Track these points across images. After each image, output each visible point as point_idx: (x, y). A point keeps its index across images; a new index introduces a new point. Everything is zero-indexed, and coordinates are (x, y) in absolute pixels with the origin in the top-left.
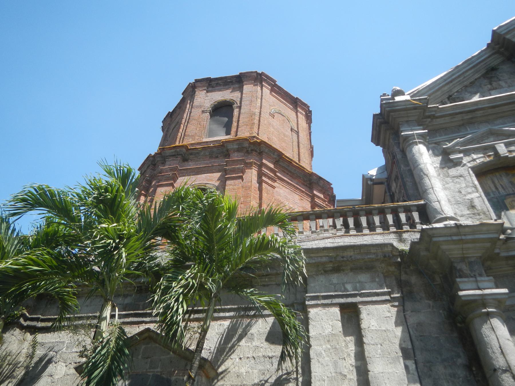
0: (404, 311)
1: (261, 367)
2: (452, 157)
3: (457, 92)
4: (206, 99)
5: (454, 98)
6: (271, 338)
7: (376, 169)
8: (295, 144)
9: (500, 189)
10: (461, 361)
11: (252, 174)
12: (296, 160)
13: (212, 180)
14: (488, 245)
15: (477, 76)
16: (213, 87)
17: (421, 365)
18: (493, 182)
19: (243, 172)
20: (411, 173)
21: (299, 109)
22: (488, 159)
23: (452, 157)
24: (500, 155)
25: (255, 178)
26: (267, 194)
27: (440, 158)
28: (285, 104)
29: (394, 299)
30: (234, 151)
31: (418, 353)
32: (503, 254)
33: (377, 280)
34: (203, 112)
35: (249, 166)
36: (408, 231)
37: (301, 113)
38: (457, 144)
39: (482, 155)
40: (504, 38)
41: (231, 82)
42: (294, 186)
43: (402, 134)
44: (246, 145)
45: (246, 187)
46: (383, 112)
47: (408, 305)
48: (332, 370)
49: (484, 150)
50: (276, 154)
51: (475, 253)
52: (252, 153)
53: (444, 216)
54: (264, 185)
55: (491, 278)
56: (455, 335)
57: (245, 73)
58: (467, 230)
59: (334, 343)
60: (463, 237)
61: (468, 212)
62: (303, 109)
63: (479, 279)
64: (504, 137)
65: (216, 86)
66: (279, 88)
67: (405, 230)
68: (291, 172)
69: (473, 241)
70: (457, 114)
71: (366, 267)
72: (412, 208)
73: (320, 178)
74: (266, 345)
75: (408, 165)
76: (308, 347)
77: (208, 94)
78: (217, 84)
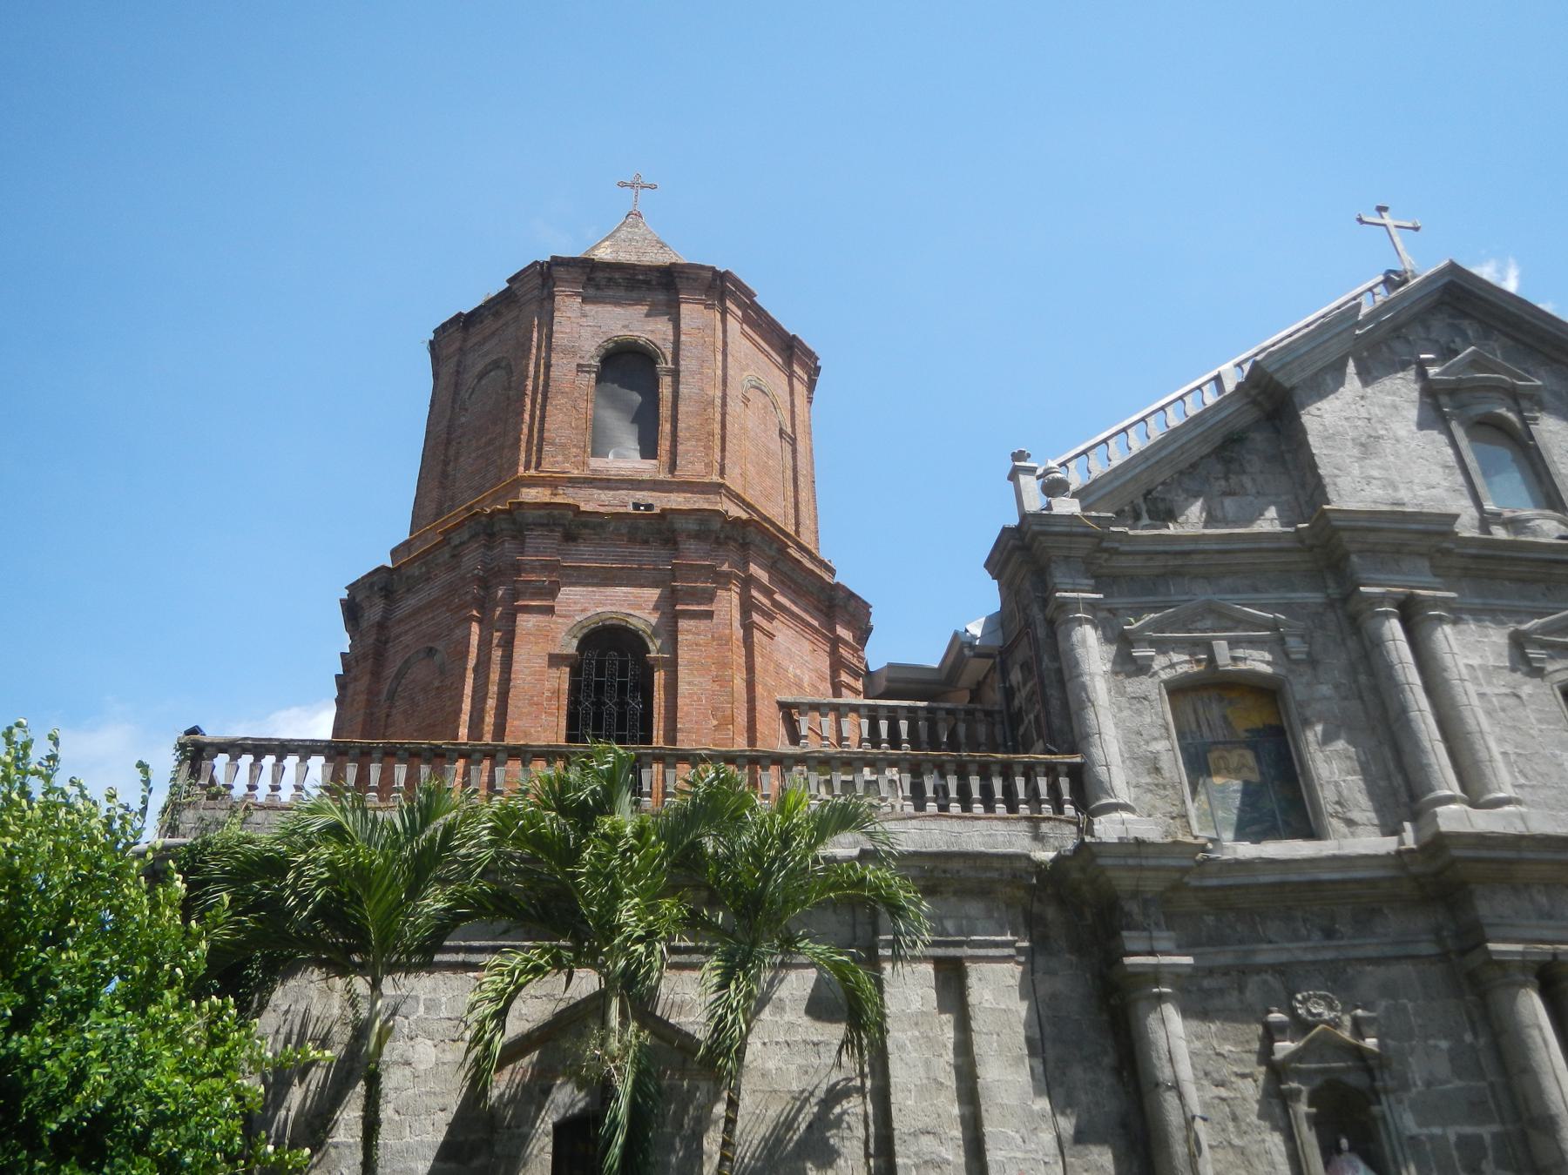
0: (1033, 972)
1: (800, 1061)
2: (1137, 653)
3: (1163, 483)
4: (584, 327)
6: (818, 1008)
8: (789, 473)
9: (1205, 728)
10: (1108, 1060)
11: (728, 603)
12: (791, 530)
13: (640, 607)
14: (1176, 876)
15: (1206, 450)
16: (598, 287)
18: (1195, 711)
19: (710, 597)
20: (1062, 683)
21: (796, 368)
22: (1196, 669)
23: (1137, 653)
24: (1217, 667)
25: (737, 616)
26: (763, 656)
27: (1114, 648)
28: (768, 355)
29: (1020, 951)
30: (689, 536)
31: (1048, 1045)
32: (1194, 883)
34: (580, 368)
35: (723, 580)
36: (1049, 819)
37: (800, 379)
38: (1146, 626)
39: (1187, 658)
41: (647, 282)
42: (803, 620)
44: (716, 525)
45: (720, 638)
46: (1025, 528)
47: (1040, 961)
48: (922, 1073)
49: (1192, 646)
50: (775, 546)
51: (1153, 885)
53: (1113, 801)
54: (757, 633)
55: (1172, 934)
56: (1105, 1017)
59: (926, 1028)
60: (1144, 862)
61: (1148, 780)
62: (804, 366)
63: (1155, 934)
64: (1230, 624)
65: (607, 286)
66: (759, 311)
67: (1045, 815)
68: (796, 583)
69: (1157, 869)
71: (982, 891)
73: (852, 595)
74: (806, 1020)
75: (1056, 656)
76: (883, 1031)
77: (587, 308)
78: (610, 280)
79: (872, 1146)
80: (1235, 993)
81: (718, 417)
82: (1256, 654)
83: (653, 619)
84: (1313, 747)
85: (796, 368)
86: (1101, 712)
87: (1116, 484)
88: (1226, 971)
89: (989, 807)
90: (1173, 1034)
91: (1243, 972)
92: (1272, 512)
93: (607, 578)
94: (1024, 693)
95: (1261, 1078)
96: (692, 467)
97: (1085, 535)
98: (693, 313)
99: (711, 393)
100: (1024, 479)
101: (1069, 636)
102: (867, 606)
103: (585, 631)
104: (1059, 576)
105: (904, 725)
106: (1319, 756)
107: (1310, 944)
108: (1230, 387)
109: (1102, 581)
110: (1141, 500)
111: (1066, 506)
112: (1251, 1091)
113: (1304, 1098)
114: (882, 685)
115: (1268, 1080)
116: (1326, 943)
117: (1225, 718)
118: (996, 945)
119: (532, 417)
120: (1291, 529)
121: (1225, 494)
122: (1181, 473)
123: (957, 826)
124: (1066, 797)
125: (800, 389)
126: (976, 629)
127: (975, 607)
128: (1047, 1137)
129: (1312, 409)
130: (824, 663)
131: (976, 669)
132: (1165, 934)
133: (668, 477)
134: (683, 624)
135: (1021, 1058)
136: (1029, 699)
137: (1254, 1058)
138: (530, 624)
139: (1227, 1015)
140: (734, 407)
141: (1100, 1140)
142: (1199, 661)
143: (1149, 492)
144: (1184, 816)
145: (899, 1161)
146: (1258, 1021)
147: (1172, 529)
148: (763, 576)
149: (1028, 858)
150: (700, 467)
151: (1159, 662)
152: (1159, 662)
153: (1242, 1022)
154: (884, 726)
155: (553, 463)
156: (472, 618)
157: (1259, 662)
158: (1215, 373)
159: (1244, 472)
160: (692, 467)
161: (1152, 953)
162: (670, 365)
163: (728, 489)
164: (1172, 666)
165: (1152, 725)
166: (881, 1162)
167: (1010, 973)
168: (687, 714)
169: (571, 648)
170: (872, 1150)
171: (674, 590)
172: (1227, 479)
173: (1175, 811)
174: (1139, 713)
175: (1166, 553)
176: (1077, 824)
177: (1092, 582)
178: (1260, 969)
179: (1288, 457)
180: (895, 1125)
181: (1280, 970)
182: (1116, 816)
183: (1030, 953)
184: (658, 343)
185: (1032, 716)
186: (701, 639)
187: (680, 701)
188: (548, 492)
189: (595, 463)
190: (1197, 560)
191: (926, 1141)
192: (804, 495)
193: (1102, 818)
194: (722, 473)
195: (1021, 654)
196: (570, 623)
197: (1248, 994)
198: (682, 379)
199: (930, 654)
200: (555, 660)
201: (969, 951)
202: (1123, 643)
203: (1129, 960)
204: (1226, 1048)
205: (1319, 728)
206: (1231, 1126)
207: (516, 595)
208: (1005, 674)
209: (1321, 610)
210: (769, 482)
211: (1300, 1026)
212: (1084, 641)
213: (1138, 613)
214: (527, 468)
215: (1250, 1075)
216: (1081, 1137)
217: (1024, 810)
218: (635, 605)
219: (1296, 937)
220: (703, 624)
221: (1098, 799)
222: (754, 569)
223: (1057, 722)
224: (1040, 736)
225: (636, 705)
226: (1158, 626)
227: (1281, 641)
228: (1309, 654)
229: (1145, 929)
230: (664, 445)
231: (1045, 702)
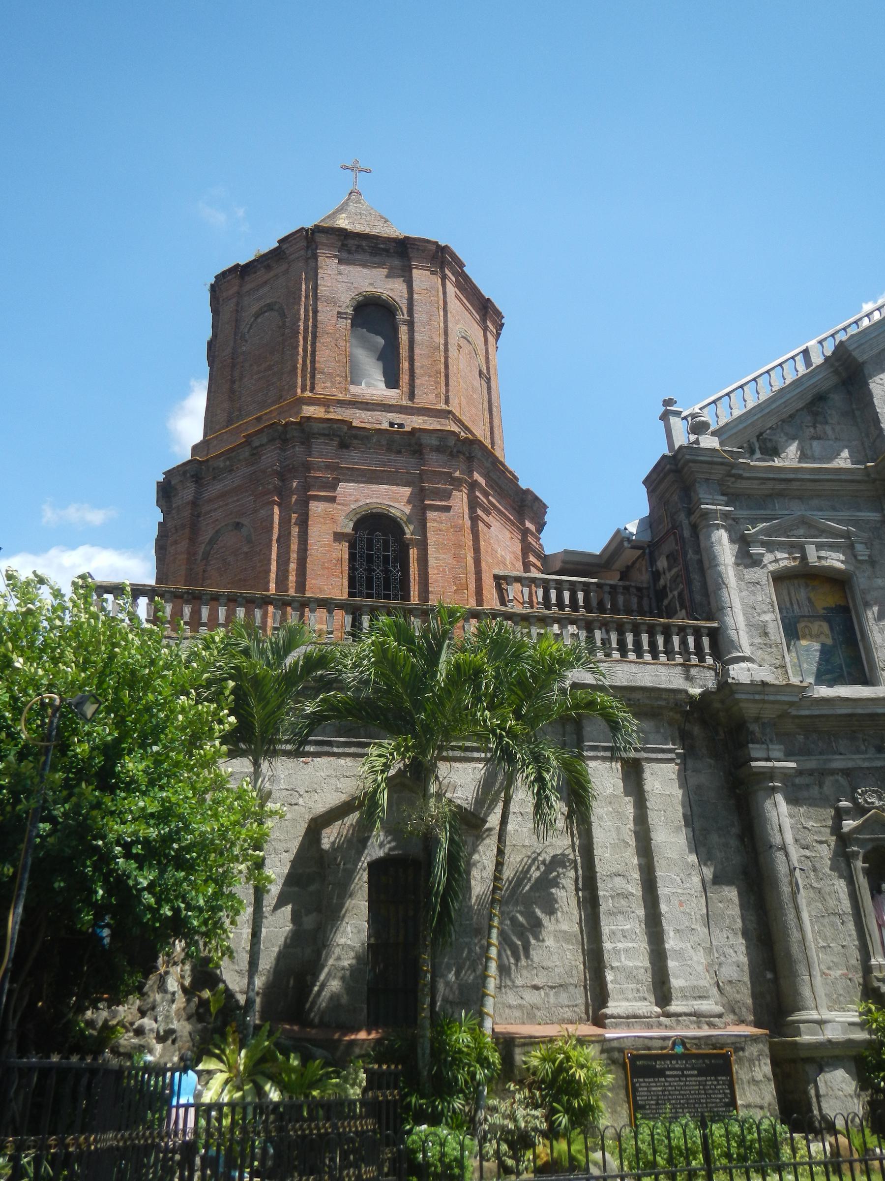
0: (685, 770)
2: (754, 550)
3: (770, 428)
4: (342, 283)
5: (765, 439)
7: (637, 521)
8: (486, 405)
9: (796, 607)
10: (735, 830)
11: (460, 500)
13: (398, 501)
14: (786, 707)
15: (801, 405)
17: (697, 833)
18: (789, 594)
19: (448, 495)
20: (702, 571)
21: (489, 324)
22: (793, 564)
24: (807, 563)
26: (485, 541)
30: (432, 450)
33: (662, 731)
35: (457, 483)
36: (696, 665)
37: (491, 332)
39: (787, 556)
40: (850, 355)
41: (387, 251)
42: (505, 515)
43: (702, 506)
44: (452, 442)
46: (679, 456)
48: (615, 836)
49: (791, 547)
50: (490, 459)
51: (769, 713)
52: (458, 457)
53: (741, 654)
54: (481, 524)
55: (782, 747)
57: (415, 239)
58: (772, 689)
60: (766, 698)
62: (494, 323)
63: (771, 746)
64: (816, 533)
65: (356, 251)
66: (466, 278)
67: (693, 662)
68: (500, 488)
70: (770, 479)
72: (702, 630)
73: (536, 499)
75: (698, 550)
77: (342, 267)
78: (358, 246)
79: (580, 883)
80: (817, 788)
81: (443, 360)
82: (834, 555)
83: (407, 510)
84: (871, 622)
85: (489, 324)
86: (732, 592)
87: (741, 427)
88: (811, 772)
89: (655, 657)
90: (781, 815)
91: (822, 774)
92: (845, 453)
93: (372, 478)
94: (669, 576)
95: (833, 844)
96: (426, 397)
97: (722, 464)
98: (422, 277)
99: (437, 340)
100: (673, 420)
101: (710, 537)
102: (545, 507)
103: (358, 516)
104: (702, 492)
105: (580, 595)
106: (875, 628)
107: (867, 756)
108: (817, 360)
109: (732, 498)
110: (754, 440)
111: (709, 442)
112: (825, 852)
113: (861, 857)
114: (558, 566)
115: (836, 845)
116: (878, 756)
117: (809, 599)
118: (663, 751)
119: (305, 350)
120: (862, 467)
121: (813, 438)
122: (783, 421)
123: (634, 668)
124: (707, 651)
125: (491, 339)
126: (632, 528)
127: (631, 513)
128: (696, 880)
129: (877, 379)
130: (517, 547)
131: (630, 555)
132: (777, 747)
133: (409, 404)
134: (430, 515)
135: (680, 828)
136: (674, 580)
137: (828, 830)
138: (320, 509)
139: (812, 803)
140: (453, 352)
141: (730, 883)
142: (795, 558)
143: (761, 434)
144: (784, 667)
145: (601, 893)
146: (831, 806)
147: (777, 462)
148: (482, 481)
149: (686, 692)
150: (432, 397)
151: (768, 558)
152: (768, 558)
153: (821, 807)
154: (553, 593)
155: (324, 388)
156: (274, 502)
157: (835, 560)
158: (804, 347)
159: (827, 423)
160: (426, 397)
161: (768, 759)
162: (406, 317)
163: (454, 415)
164: (776, 561)
165: (763, 602)
166: (586, 893)
167: (670, 770)
168: (436, 581)
169: (348, 528)
170: (580, 886)
171: (422, 489)
172: (815, 427)
173: (778, 663)
174: (753, 593)
175: (774, 479)
176: (715, 670)
177: (725, 498)
178: (833, 772)
179: (857, 413)
180: (597, 870)
181: (846, 772)
182: (743, 665)
183: (683, 757)
184: (397, 299)
185: (676, 593)
186: (443, 526)
187: (430, 571)
188: (322, 410)
189: (354, 389)
190: (795, 485)
191: (618, 880)
192: (496, 422)
193: (735, 666)
194: (447, 402)
195: (670, 546)
196: (348, 509)
197: (825, 788)
198: (416, 329)
199: (594, 543)
200: (338, 537)
201: (645, 755)
202: (743, 542)
203: (753, 764)
204: (810, 824)
205: (876, 609)
206: (812, 874)
207: (306, 487)
208: (653, 561)
209: (878, 526)
210: (474, 411)
211: (860, 810)
212: (720, 541)
213: (754, 522)
214: (303, 390)
215: (825, 842)
216: (718, 880)
217: (679, 659)
218: (395, 499)
219: (858, 751)
220: (444, 516)
221: (730, 653)
222: (476, 476)
223: (698, 598)
224: (683, 606)
225: (396, 572)
226: (767, 532)
227: (852, 546)
228: (870, 556)
229: (763, 743)
230: (405, 378)
231: (689, 582)
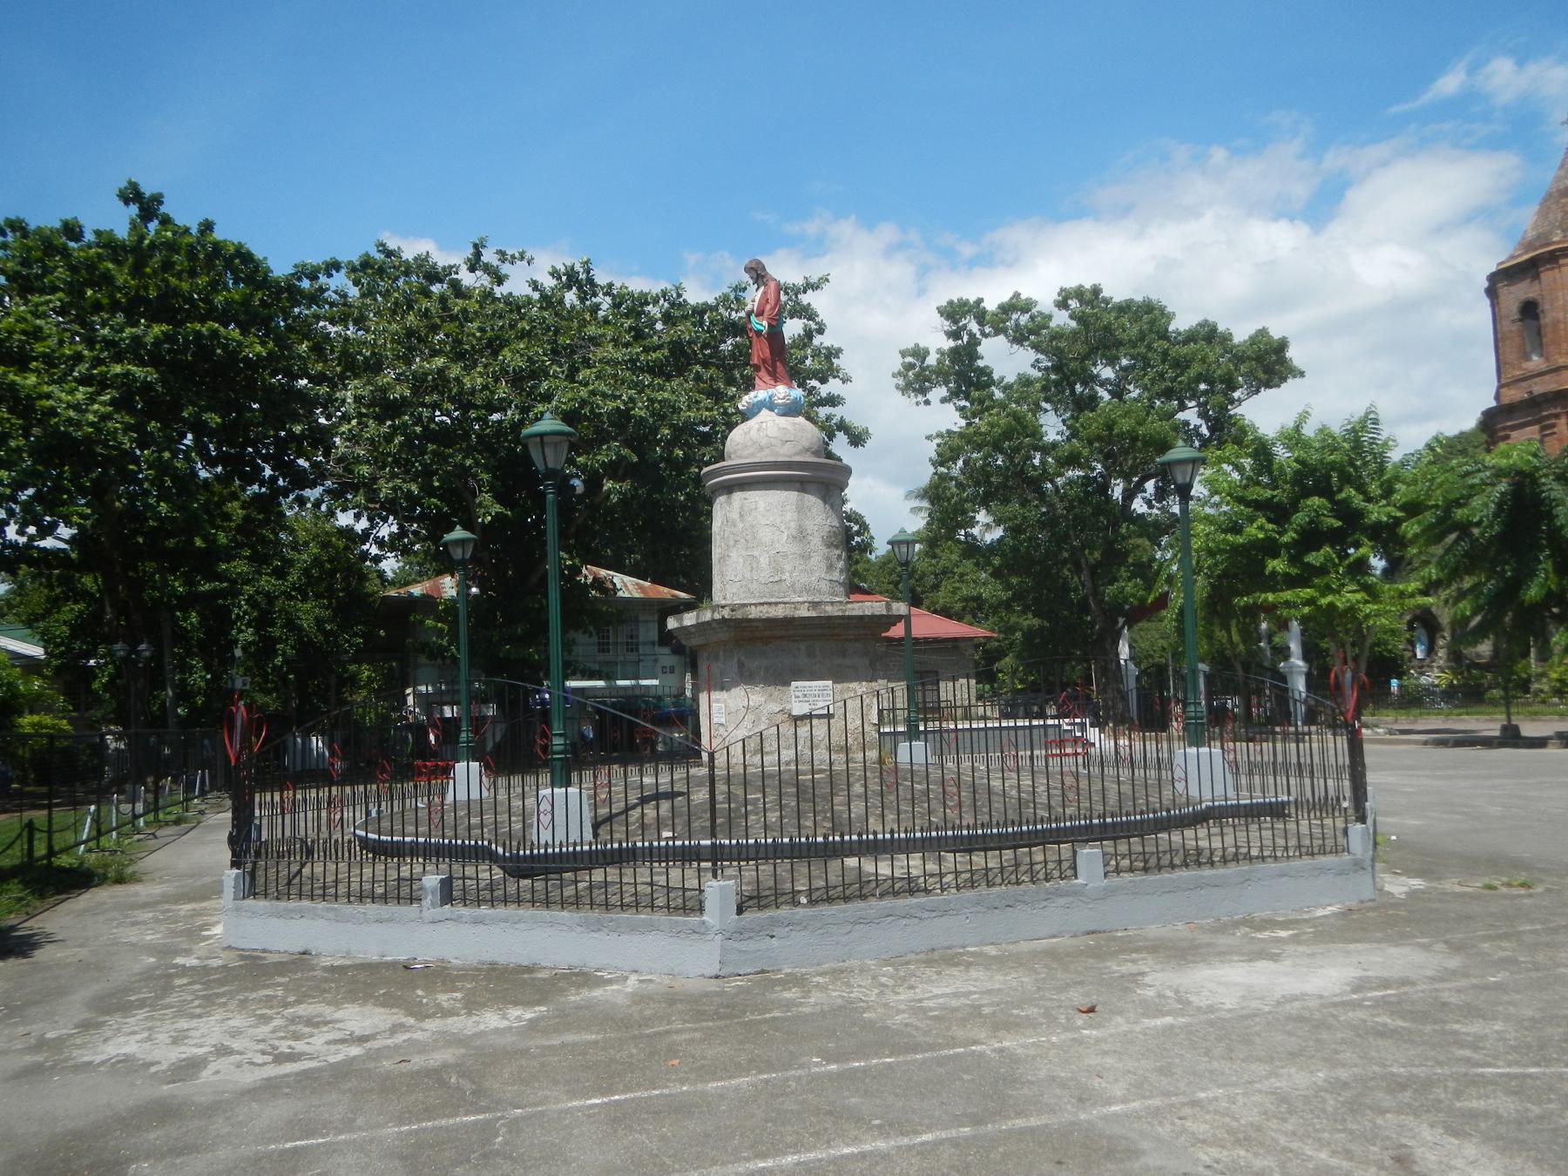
19: (1553, 426)
35: (1557, 416)
